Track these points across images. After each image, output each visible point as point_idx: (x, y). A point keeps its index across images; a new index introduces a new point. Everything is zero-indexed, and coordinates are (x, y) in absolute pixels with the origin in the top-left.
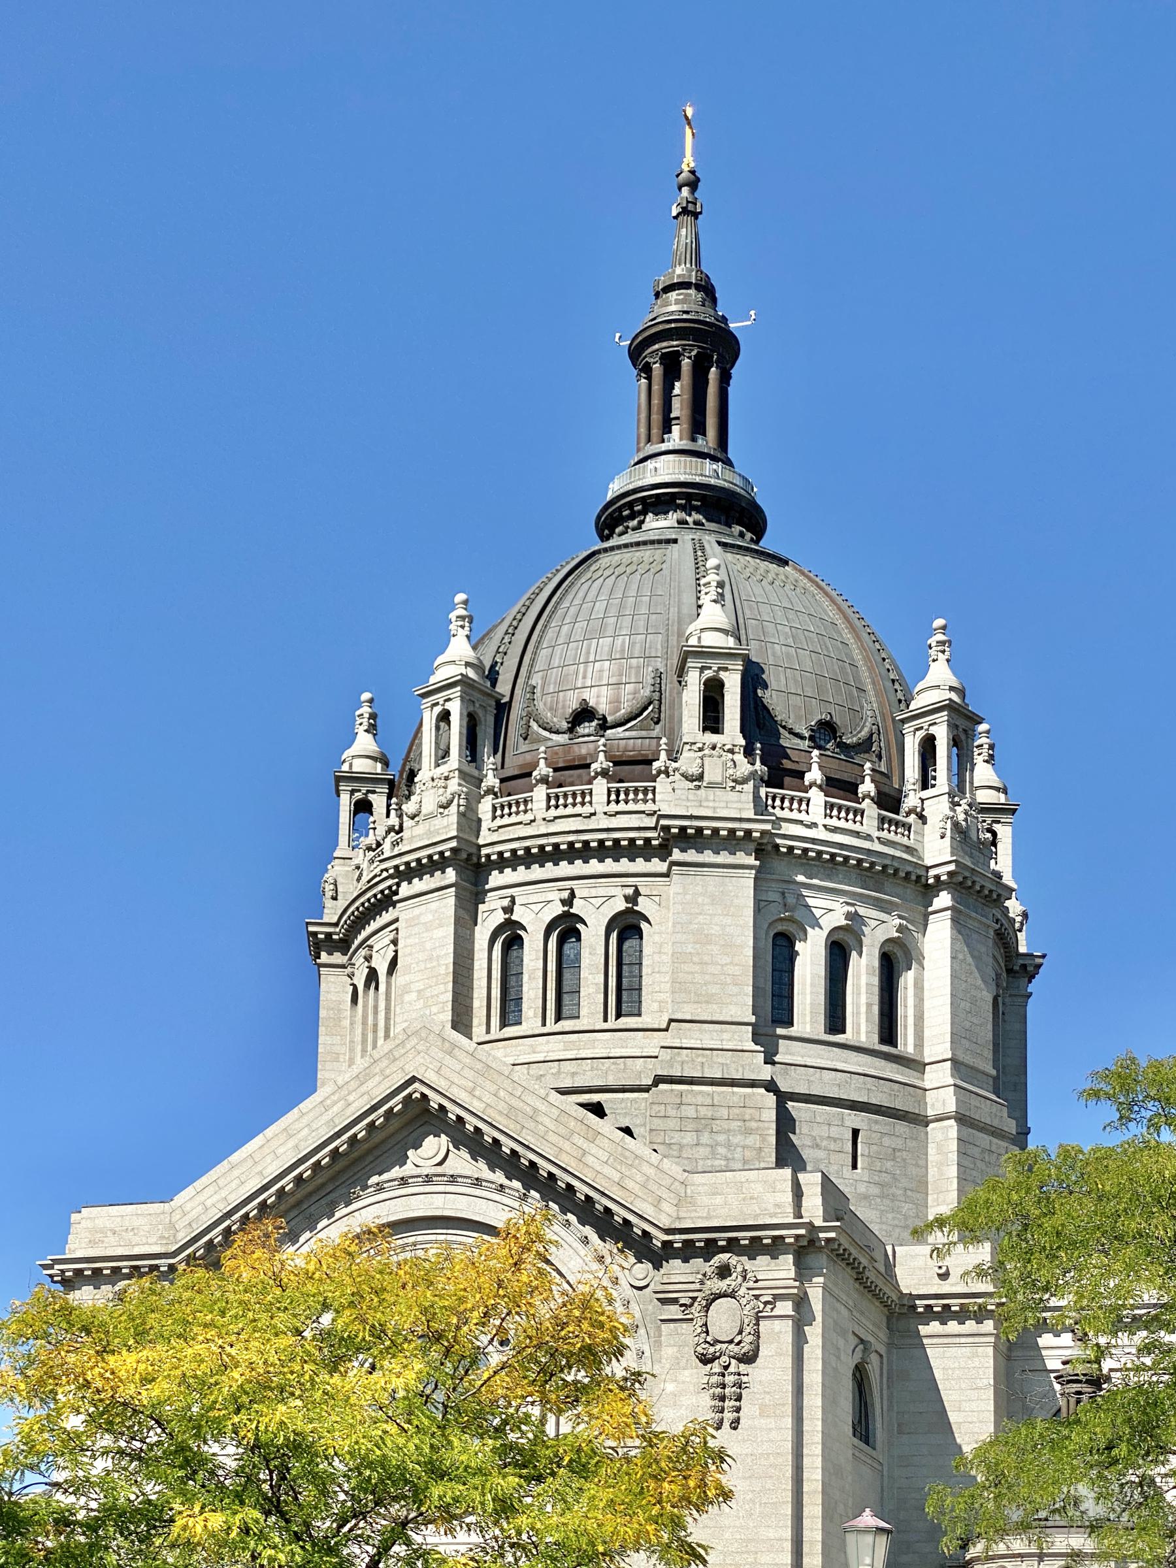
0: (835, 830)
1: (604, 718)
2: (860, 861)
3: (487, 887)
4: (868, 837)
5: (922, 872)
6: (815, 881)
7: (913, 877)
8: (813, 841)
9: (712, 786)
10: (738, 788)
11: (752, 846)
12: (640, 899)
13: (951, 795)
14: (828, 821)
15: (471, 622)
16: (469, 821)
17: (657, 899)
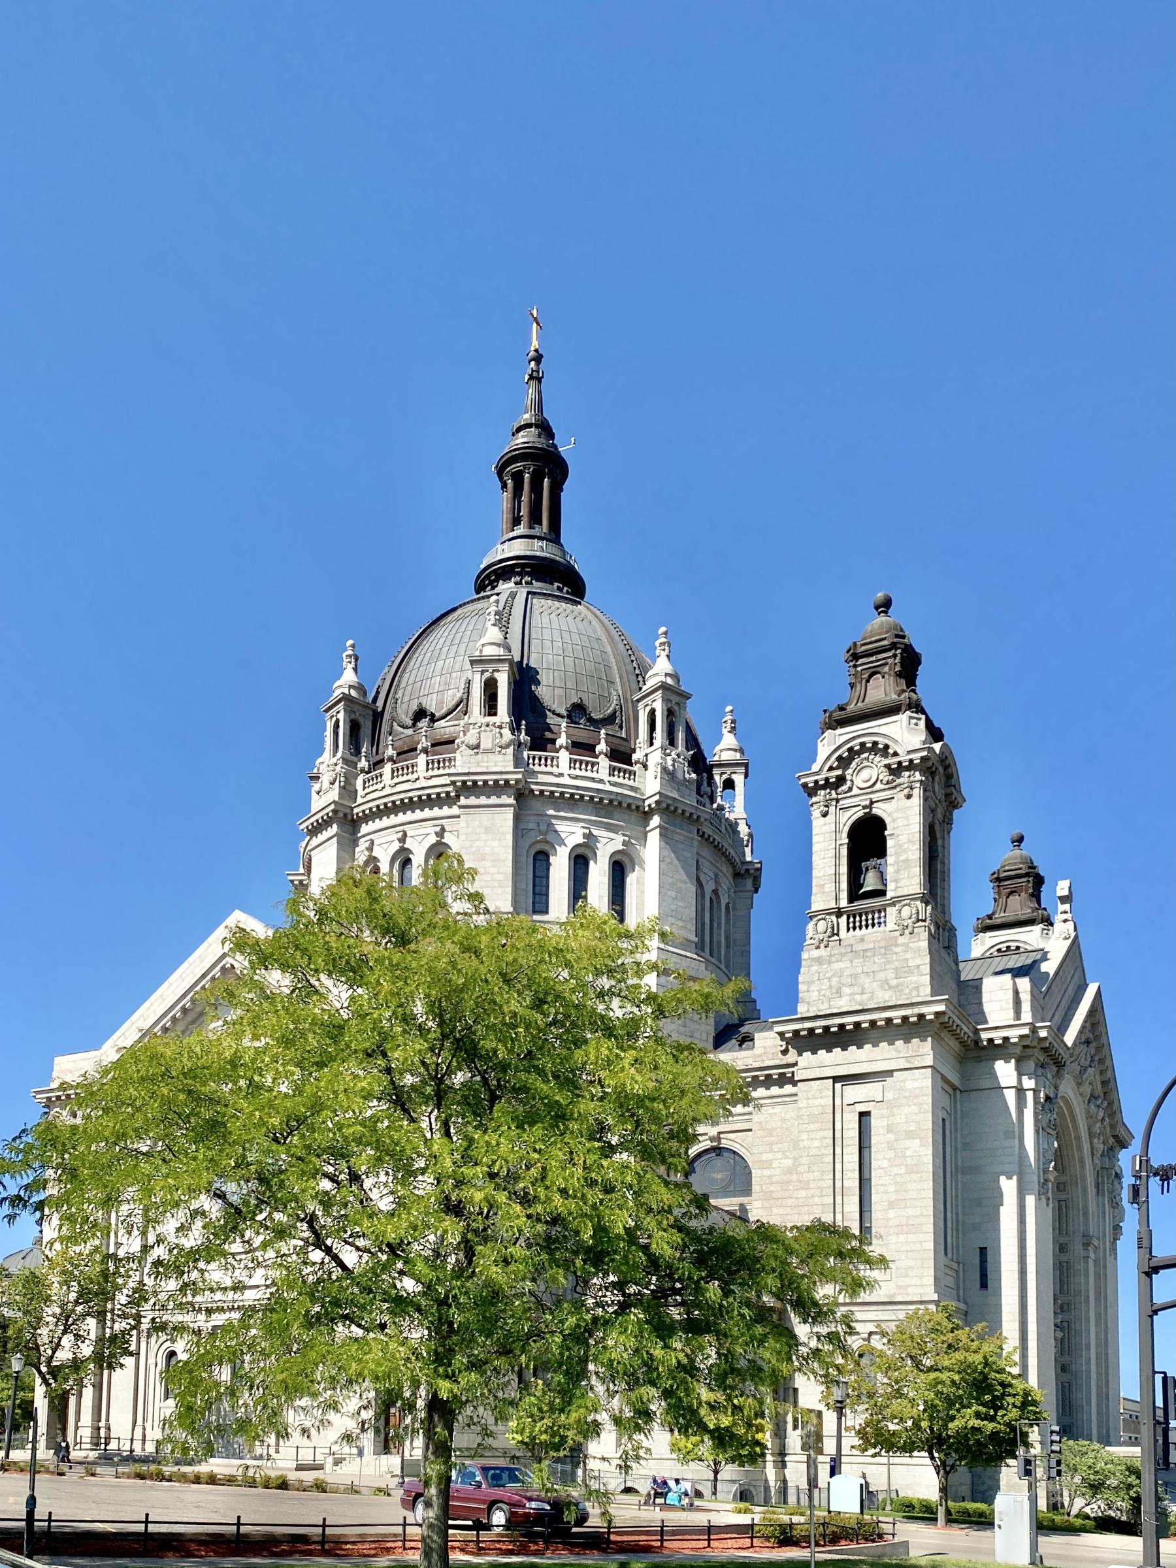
0: (576, 777)
1: (433, 715)
2: (592, 798)
3: (359, 835)
4: (601, 781)
5: (640, 803)
6: (562, 814)
7: (634, 807)
8: (558, 785)
9: (486, 752)
10: (503, 751)
11: (512, 791)
12: (446, 834)
13: (663, 748)
14: (572, 772)
15: (356, 660)
16: (348, 790)
17: (456, 833)
